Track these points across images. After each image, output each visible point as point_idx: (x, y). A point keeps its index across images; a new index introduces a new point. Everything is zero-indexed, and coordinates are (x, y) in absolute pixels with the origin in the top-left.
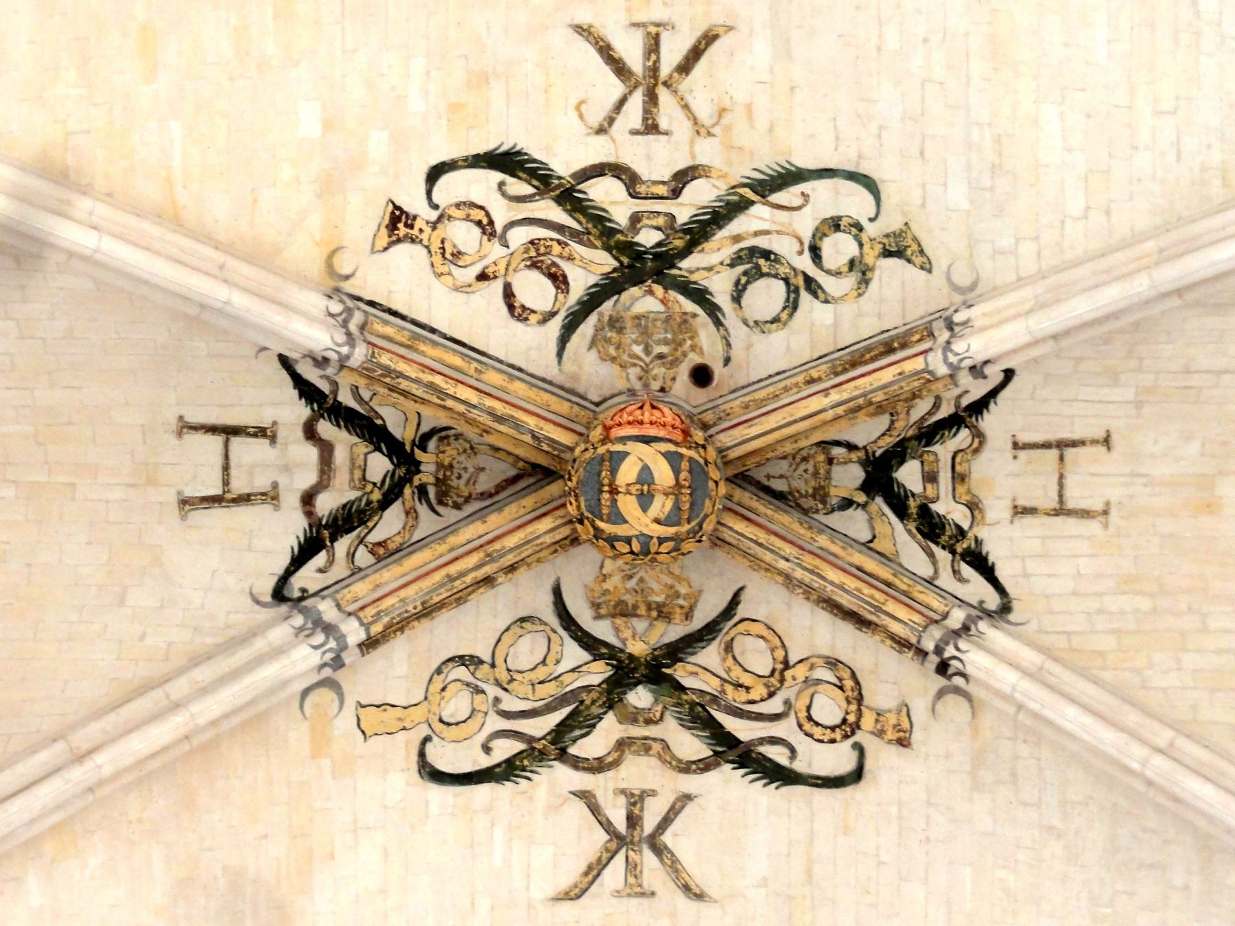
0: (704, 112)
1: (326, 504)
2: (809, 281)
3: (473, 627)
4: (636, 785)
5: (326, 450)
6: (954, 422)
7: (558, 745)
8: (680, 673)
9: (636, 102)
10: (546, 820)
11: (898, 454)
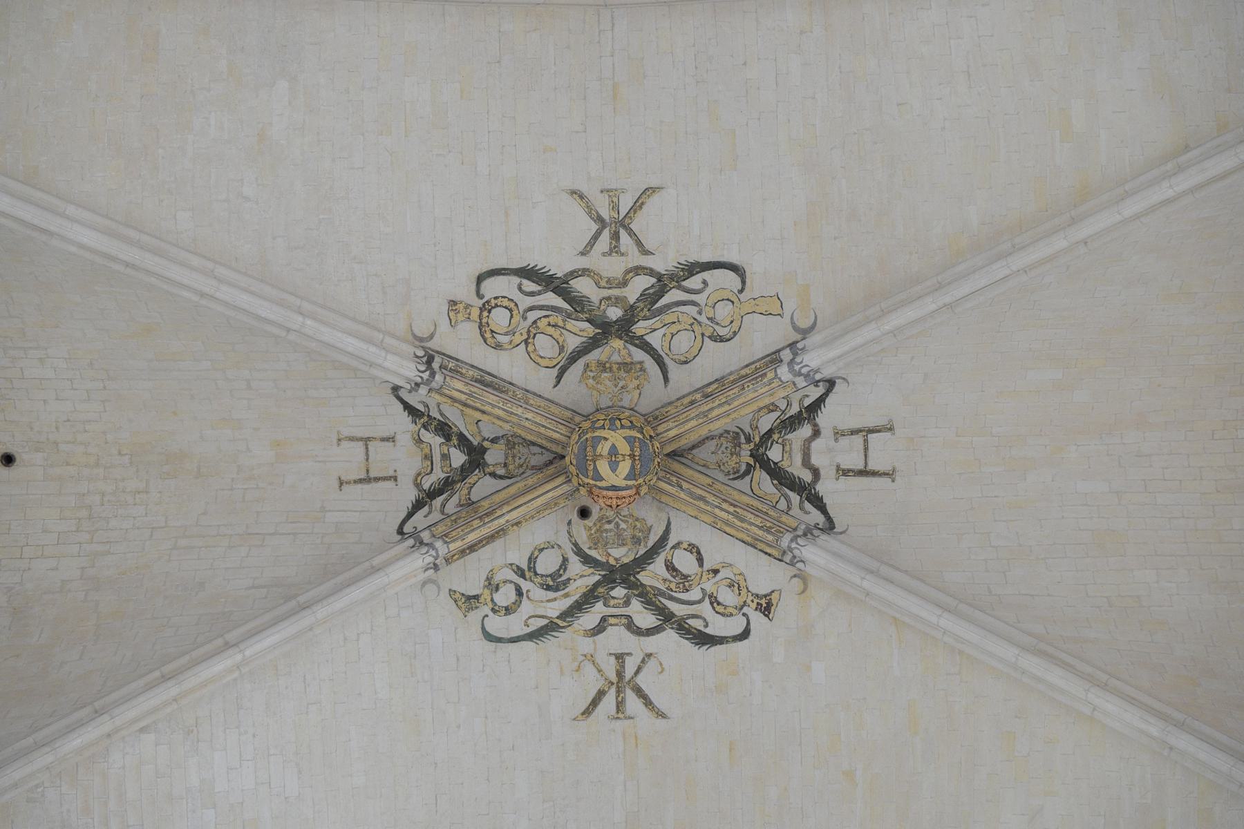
0: (589, 669)
1: (806, 431)
2: (523, 576)
3: (715, 361)
4: (615, 258)
5: (806, 463)
6: (432, 494)
7: (663, 283)
8: (590, 330)
9: (629, 673)
10: (669, 236)
11: (465, 471)
